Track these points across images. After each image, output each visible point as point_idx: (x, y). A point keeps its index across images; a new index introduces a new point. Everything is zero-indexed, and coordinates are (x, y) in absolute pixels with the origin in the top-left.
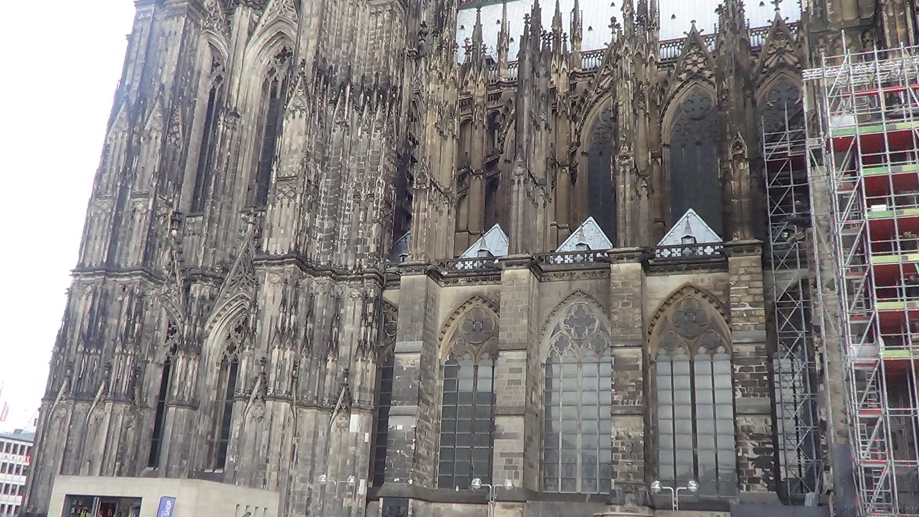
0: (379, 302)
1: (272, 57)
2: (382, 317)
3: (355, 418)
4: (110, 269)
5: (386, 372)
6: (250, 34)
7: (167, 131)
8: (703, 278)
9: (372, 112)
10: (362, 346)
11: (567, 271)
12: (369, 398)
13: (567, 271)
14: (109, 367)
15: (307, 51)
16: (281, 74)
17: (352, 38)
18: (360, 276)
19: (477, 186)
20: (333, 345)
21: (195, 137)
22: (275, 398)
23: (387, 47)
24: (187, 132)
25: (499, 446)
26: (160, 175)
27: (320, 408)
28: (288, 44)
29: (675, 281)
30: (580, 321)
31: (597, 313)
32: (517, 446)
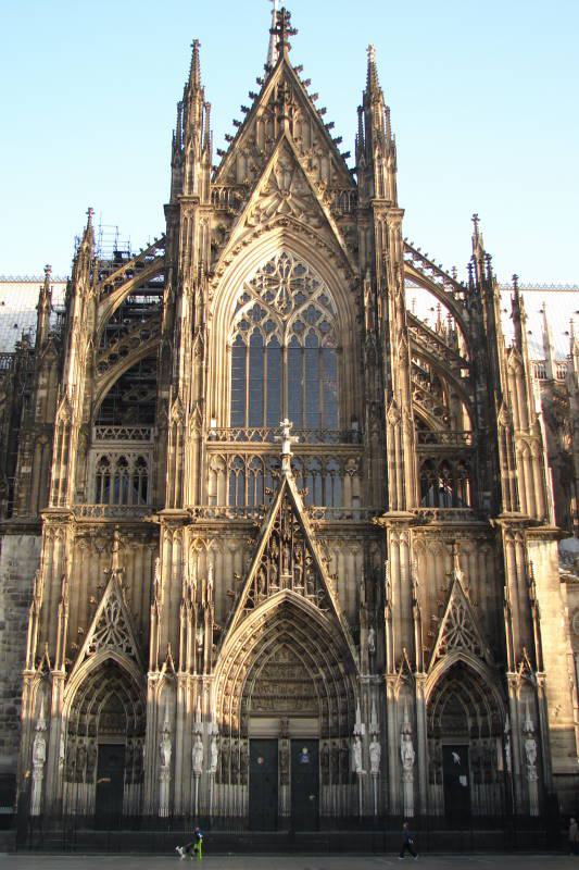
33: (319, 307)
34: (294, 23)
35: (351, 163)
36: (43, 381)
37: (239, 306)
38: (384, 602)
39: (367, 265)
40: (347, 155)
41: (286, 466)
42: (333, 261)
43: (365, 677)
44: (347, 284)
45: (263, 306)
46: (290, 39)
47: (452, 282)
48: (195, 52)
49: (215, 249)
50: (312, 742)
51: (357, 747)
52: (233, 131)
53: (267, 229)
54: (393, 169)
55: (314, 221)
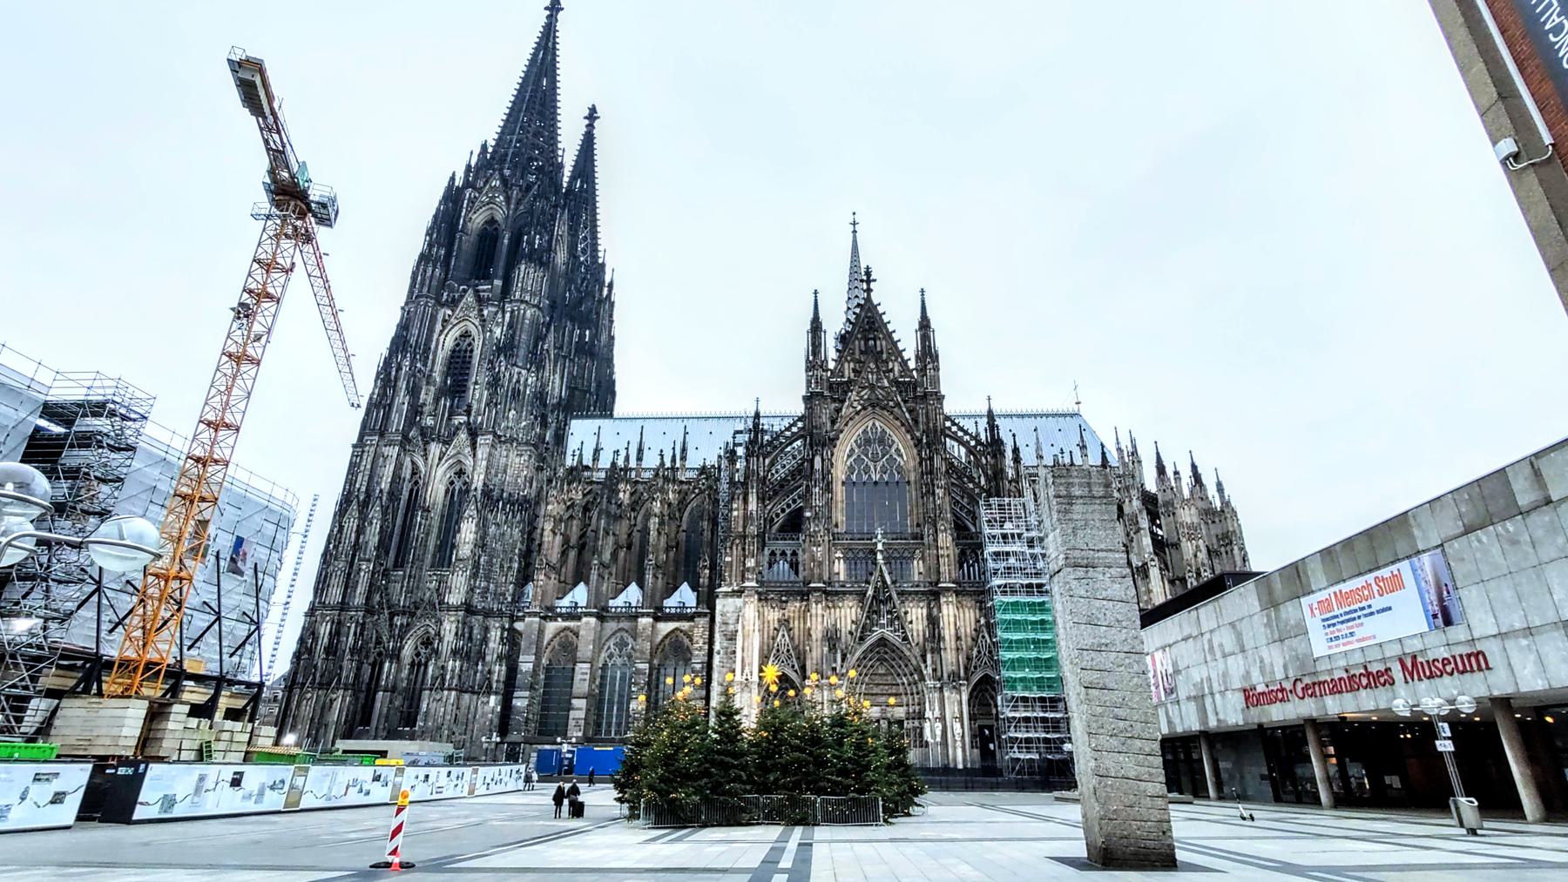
0: (512, 630)
2: (512, 639)
3: (493, 698)
4: (343, 606)
5: (512, 670)
7: (384, 520)
8: (685, 625)
10: (500, 658)
11: (617, 617)
12: (501, 686)
13: (617, 617)
14: (341, 668)
15: (478, 481)
16: (458, 485)
17: (505, 472)
18: (501, 614)
19: (572, 554)
20: (481, 656)
21: (399, 521)
22: (450, 689)
24: (394, 518)
25: (572, 714)
26: (377, 549)
27: (473, 693)
29: (671, 626)
30: (622, 644)
31: (630, 640)
32: (582, 714)
35: (912, 364)
38: (941, 638)
41: (879, 556)
43: (930, 683)
49: (833, 422)
50: (900, 723)
51: (927, 725)
53: (864, 408)
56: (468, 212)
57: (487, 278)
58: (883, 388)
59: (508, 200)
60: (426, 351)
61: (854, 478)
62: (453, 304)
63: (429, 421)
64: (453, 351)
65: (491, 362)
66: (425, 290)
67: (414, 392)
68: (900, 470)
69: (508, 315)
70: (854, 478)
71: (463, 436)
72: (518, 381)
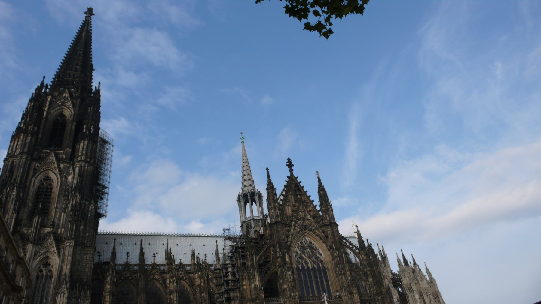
1: (42, 266)
6: (35, 255)
9: (85, 293)
15: (67, 268)
23: (91, 268)
28: (49, 260)
33: (318, 255)
34: (293, 163)
35: (318, 208)
36: (244, 283)
37: (296, 256)
39: (333, 242)
40: (316, 206)
42: (321, 241)
44: (326, 248)
45: (303, 255)
46: (293, 168)
47: (355, 246)
48: (268, 171)
52: (282, 197)
54: (332, 211)
55: (313, 228)
56: (49, 108)
57: (60, 145)
58: (308, 220)
59: (73, 105)
60: (23, 186)
61: (300, 267)
62: (40, 159)
63: (25, 230)
64: (39, 188)
65: (65, 196)
66: (26, 150)
67: (17, 211)
68: (321, 261)
69: (77, 169)
70: (300, 267)
71: (51, 240)
72: (84, 208)
